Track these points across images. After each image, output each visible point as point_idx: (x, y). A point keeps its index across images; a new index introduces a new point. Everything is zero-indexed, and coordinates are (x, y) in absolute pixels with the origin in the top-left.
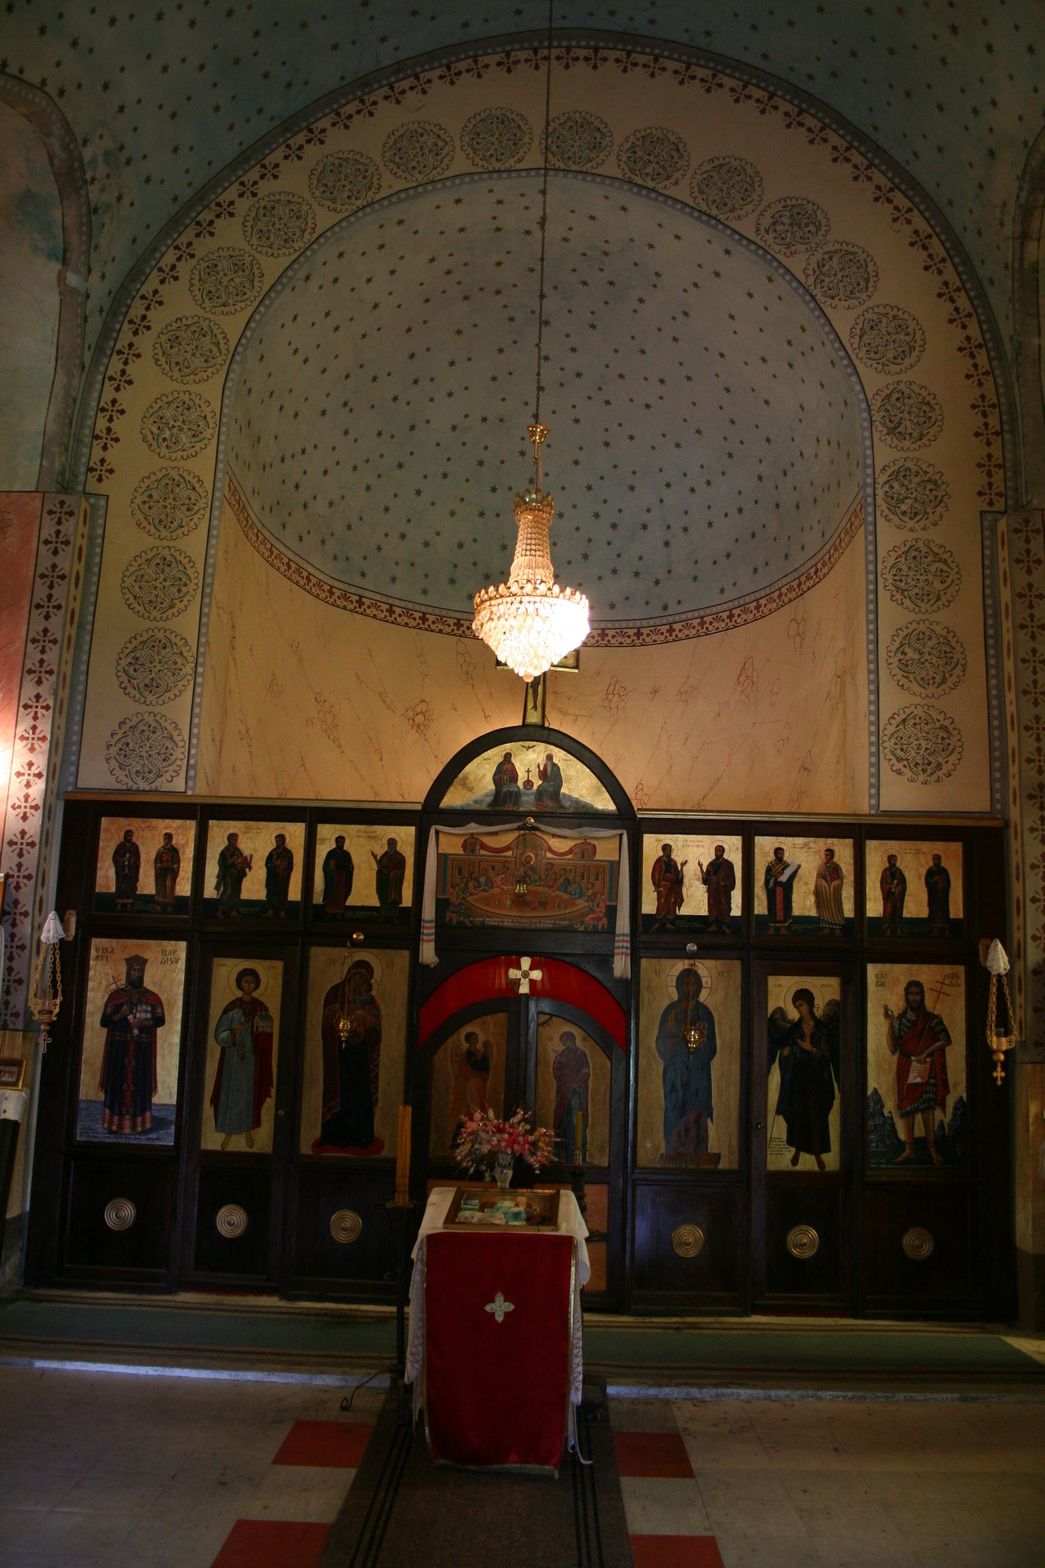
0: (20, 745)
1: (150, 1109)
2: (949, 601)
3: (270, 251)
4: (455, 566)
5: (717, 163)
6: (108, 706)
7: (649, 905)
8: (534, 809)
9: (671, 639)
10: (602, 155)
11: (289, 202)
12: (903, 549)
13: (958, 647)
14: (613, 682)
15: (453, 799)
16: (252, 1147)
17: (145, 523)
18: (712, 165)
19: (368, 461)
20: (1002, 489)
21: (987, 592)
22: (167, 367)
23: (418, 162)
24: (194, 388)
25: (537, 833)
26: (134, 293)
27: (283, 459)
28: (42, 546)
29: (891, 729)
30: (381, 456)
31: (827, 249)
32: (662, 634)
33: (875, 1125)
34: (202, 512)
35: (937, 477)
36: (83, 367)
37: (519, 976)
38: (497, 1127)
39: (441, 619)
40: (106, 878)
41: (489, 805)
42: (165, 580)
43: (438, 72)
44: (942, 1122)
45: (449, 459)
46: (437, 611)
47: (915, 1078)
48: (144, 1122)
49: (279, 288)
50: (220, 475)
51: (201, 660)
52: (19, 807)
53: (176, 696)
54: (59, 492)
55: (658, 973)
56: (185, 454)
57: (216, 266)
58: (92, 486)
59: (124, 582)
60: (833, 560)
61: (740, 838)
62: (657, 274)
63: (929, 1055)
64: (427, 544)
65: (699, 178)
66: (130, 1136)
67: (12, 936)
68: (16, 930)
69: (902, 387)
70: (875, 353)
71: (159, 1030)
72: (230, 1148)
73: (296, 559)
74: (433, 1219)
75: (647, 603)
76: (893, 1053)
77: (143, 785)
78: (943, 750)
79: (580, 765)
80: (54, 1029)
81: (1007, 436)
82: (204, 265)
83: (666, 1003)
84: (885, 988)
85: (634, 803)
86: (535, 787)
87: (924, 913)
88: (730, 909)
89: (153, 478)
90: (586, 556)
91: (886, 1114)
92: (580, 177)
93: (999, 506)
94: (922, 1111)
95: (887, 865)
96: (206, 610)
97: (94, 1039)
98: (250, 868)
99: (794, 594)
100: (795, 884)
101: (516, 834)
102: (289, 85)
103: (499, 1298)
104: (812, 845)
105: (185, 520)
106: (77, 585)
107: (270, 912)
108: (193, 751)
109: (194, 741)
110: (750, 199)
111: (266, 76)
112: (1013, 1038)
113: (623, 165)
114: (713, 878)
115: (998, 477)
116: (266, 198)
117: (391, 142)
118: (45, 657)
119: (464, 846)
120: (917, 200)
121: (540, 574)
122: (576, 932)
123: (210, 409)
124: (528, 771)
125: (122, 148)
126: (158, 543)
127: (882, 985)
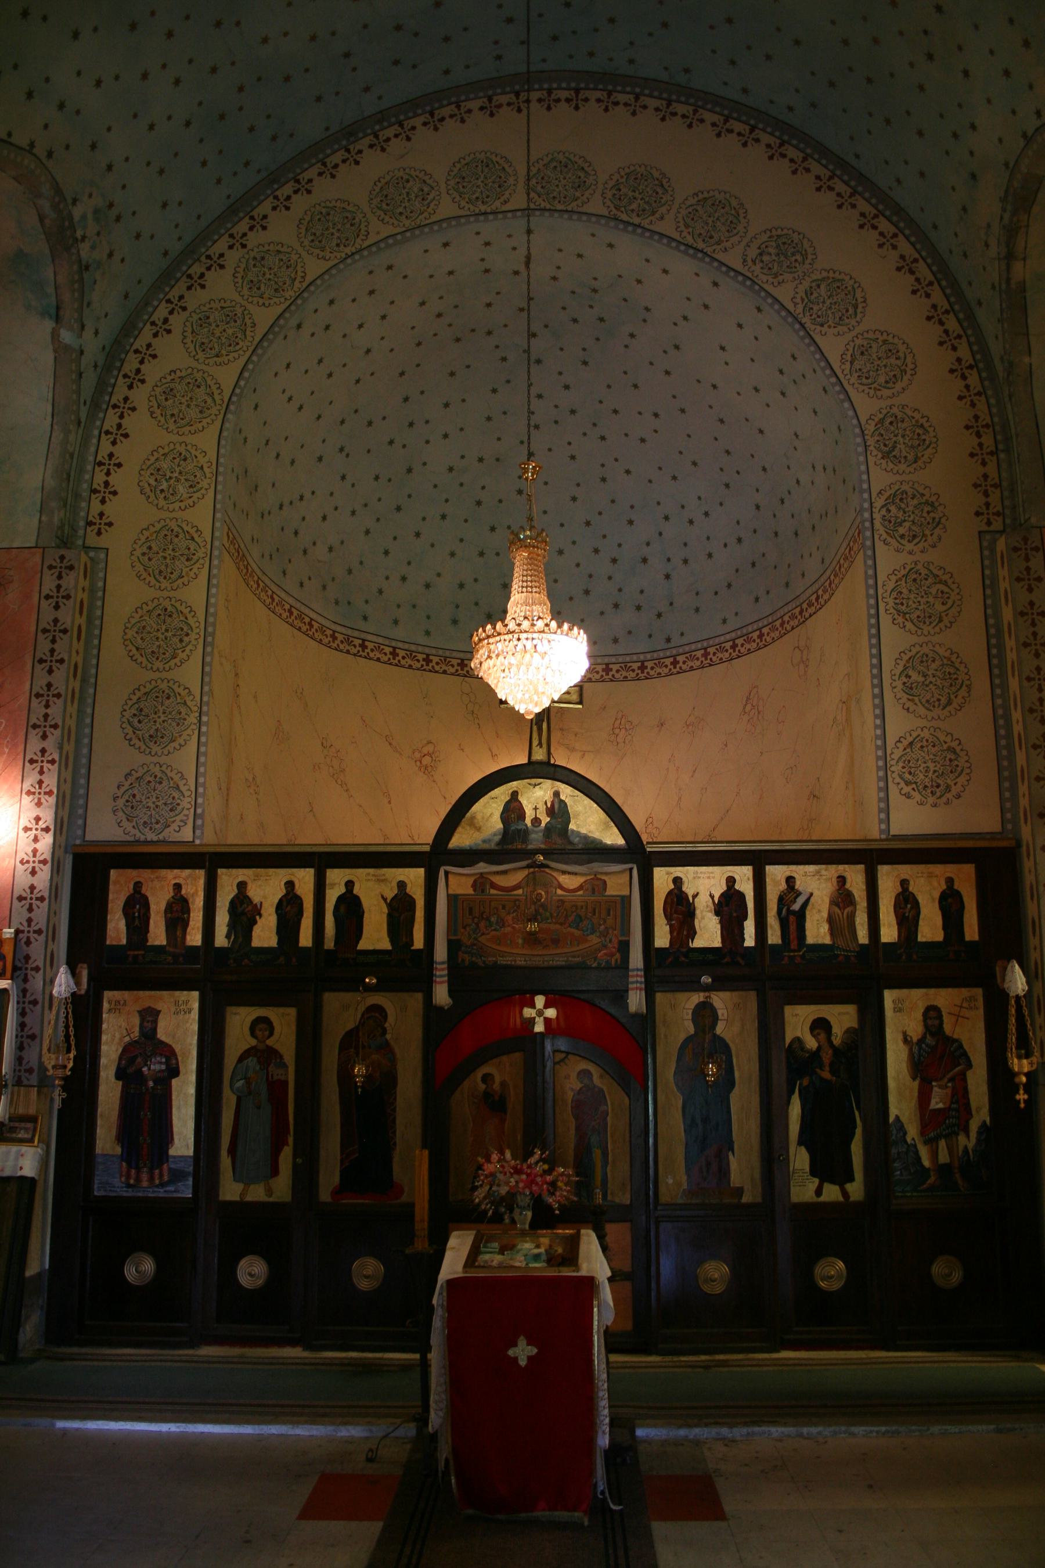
0: (26, 800)
1: (167, 1161)
2: (951, 623)
3: (261, 301)
4: (457, 606)
5: (701, 196)
6: (114, 758)
7: (662, 939)
8: (543, 846)
9: (675, 671)
10: (587, 194)
11: (279, 252)
12: (903, 572)
13: (962, 668)
14: (620, 716)
15: (462, 839)
16: (271, 1196)
17: (145, 575)
18: (696, 199)
19: (366, 505)
20: (999, 508)
21: (989, 611)
22: (162, 420)
23: (405, 207)
24: (189, 439)
25: (547, 870)
26: (128, 348)
27: (281, 507)
28: (43, 601)
29: (898, 753)
31: (814, 277)
32: (666, 666)
33: (899, 1153)
34: (201, 561)
35: (934, 499)
36: (79, 423)
37: (534, 1015)
38: (515, 1168)
39: (445, 660)
40: (117, 929)
41: (498, 844)
42: (167, 630)
43: (422, 119)
44: (966, 1147)
45: (447, 501)
46: (440, 652)
47: (937, 1103)
48: (161, 1175)
49: (271, 336)
50: (218, 524)
51: (205, 709)
52: (28, 862)
53: (181, 745)
54: (58, 547)
56: (183, 505)
57: (208, 318)
58: (92, 540)
59: (126, 634)
60: (833, 586)
61: (750, 868)
62: (647, 309)
63: (950, 1080)
64: (428, 586)
65: (684, 212)
66: (148, 1188)
67: (24, 991)
68: (28, 986)
69: (895, 410)
70: (867, 378)
71: (174, 1082)
72: (249, 1198)
73: (298, 605)
74: (453, 1264)
75: (650, 636)
76: (914, 1079)
77: (151, 836)
78: (951, 772)
79: (587, 801)
80: (68, 1084)
81: (1002, 456)
82: (195, 317)
83: (682, 1037)
84: (902, 1013)
85: (645, 838)
86: (543, 825)
87: (939, 936)
88: (743, 940)
89: (152, 529)
90: (587, 592)
91: (909, 1140)
92: (566, 216)
93: (997, 525)
94: (946, 1137)
95: (900, 890)
96: (208, 659)
97: (109, 1093)
98: (261, 916)
99: (796, 622)
100: (807, 913)
101: (526, 872)
102: (274, 138)
103: (522, 1342)
104: (824, 872)
105: (185, 570)
106: (79, 639)
107: (282, 959)
108: (200, 800)
109: (201, 790)
110: (735, 231)
111: (252, 129)
112: (1034, 1059)
113: (609, 203)
114: (725, 909)
115: (995, 496)
116: (256, 250)
117: (377, 190)
118: (49, 711)
119: (474, 886)
120: (902, 225)
121: (537, 610)
122: (590, 968)
123: (206, 459)
124: (536, 809)
125: (111, 205)
126: (159, 594)
127: (900, 1010)
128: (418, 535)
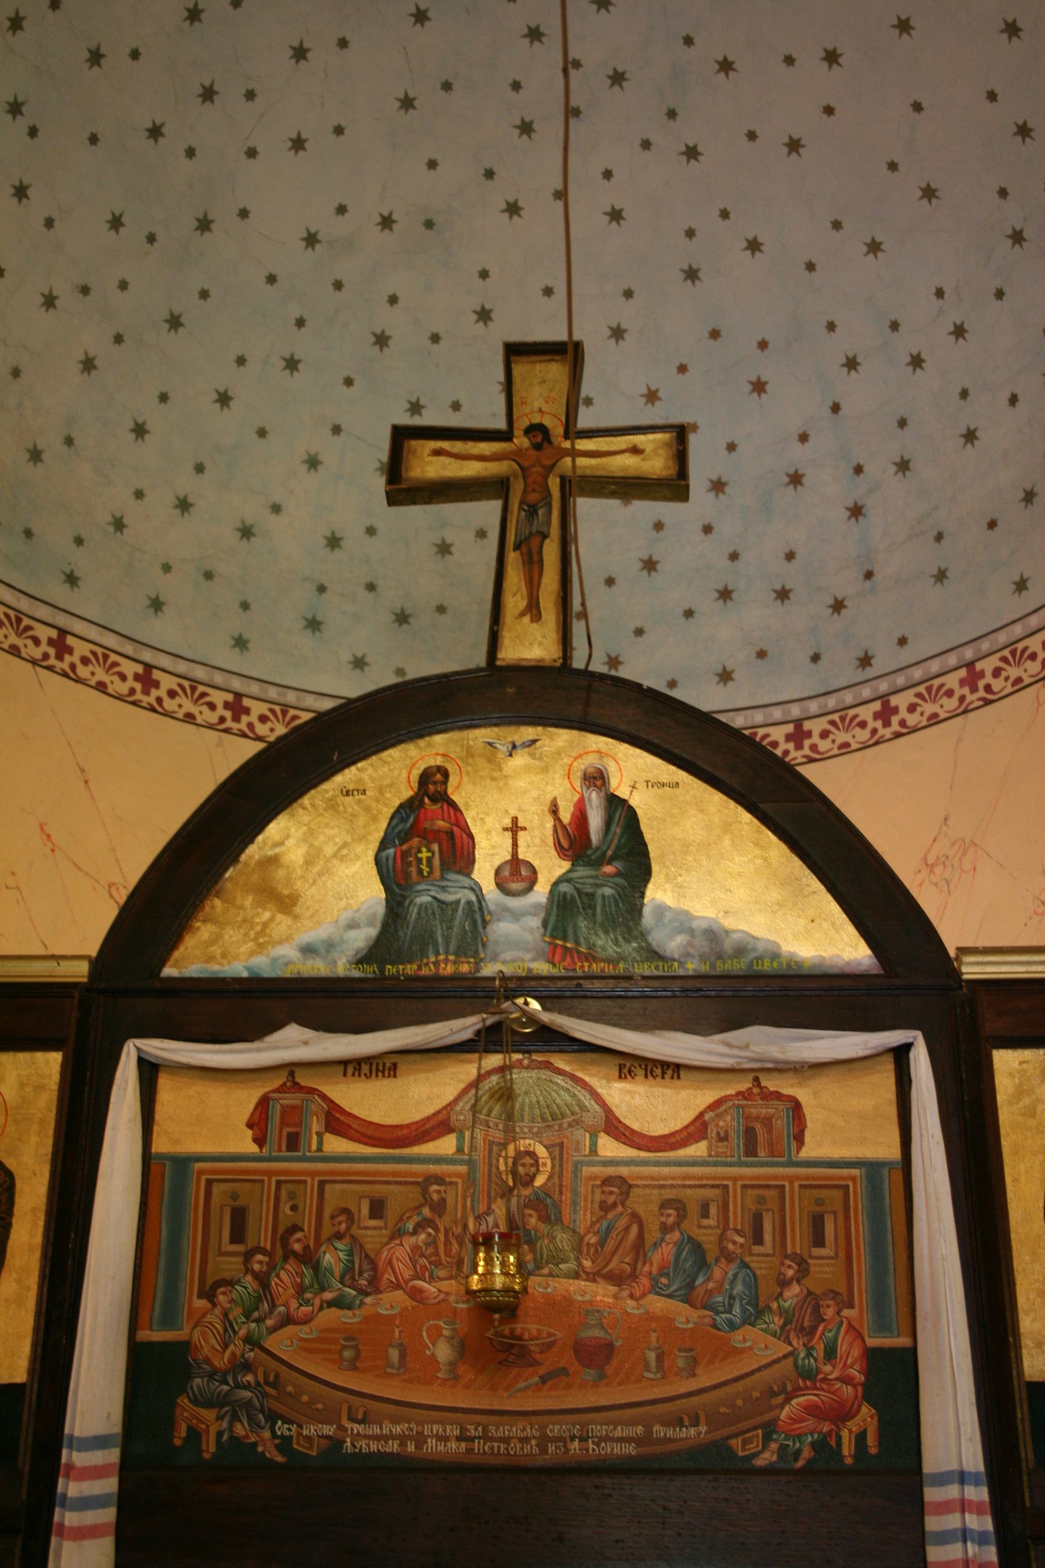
4: (322, 589)
8: (542, 968)
9: (887, 733)
15: (220, 946)
30: (123, 285)
32: (863, 725)
41: (363, 960)
45: (300, 323)
46: (273, 693)
64: (246, 532)
75: (816, 658)
86: (541, 892)
90: (650, 565)
101: (467, 1070)
119: (258, 1124)
122: (744, 1470)
128: (224, 399)
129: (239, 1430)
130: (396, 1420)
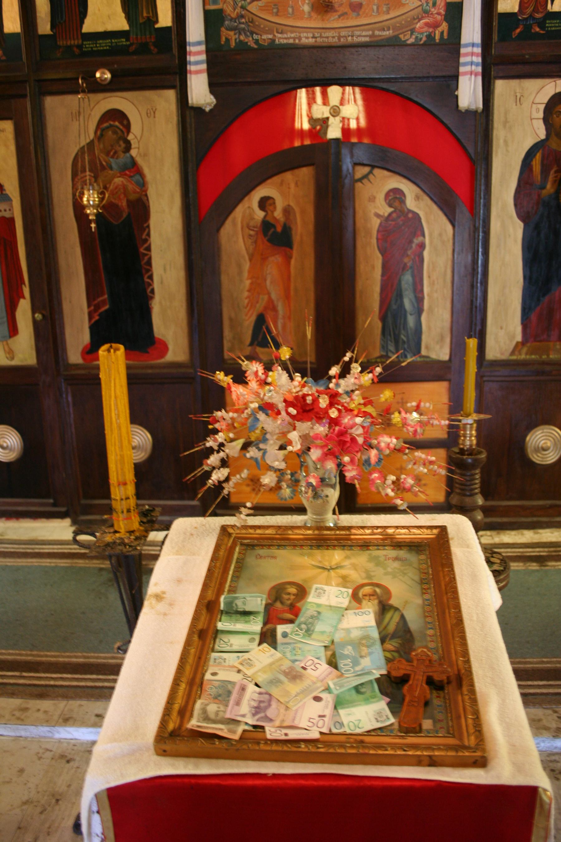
16: (12, 358)
37: (327, 115)
55: (519, 101)
122: (404, 45)
129: (242, 38)
130: (292, 32)
